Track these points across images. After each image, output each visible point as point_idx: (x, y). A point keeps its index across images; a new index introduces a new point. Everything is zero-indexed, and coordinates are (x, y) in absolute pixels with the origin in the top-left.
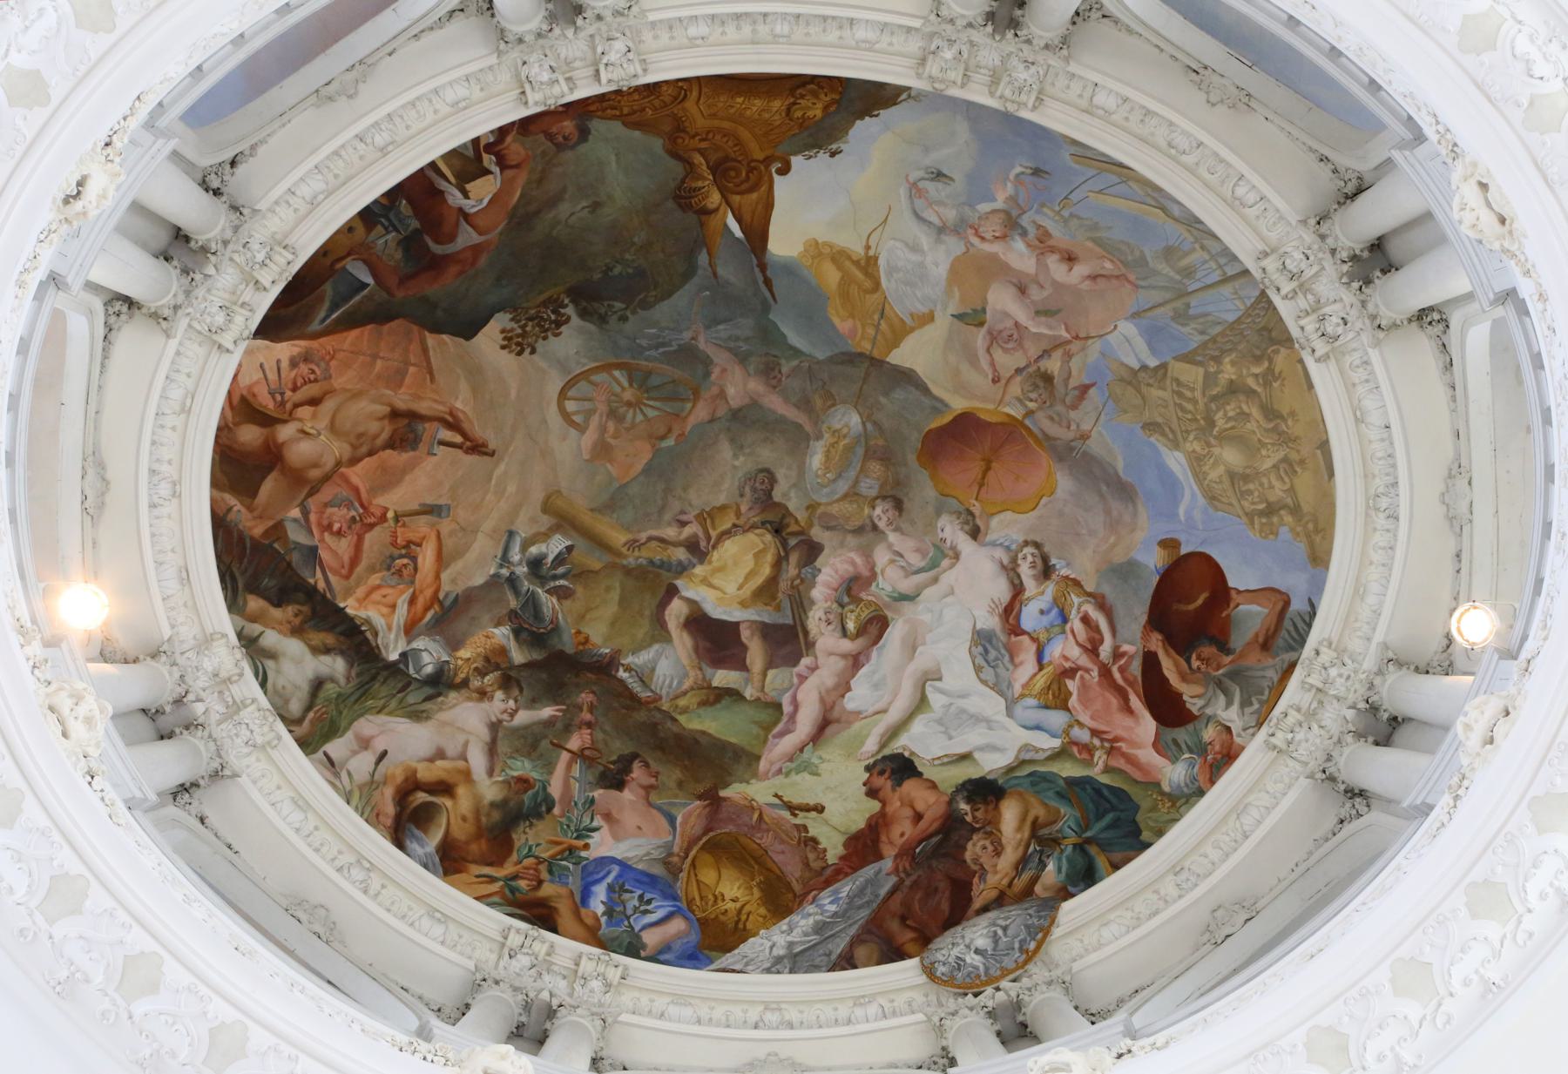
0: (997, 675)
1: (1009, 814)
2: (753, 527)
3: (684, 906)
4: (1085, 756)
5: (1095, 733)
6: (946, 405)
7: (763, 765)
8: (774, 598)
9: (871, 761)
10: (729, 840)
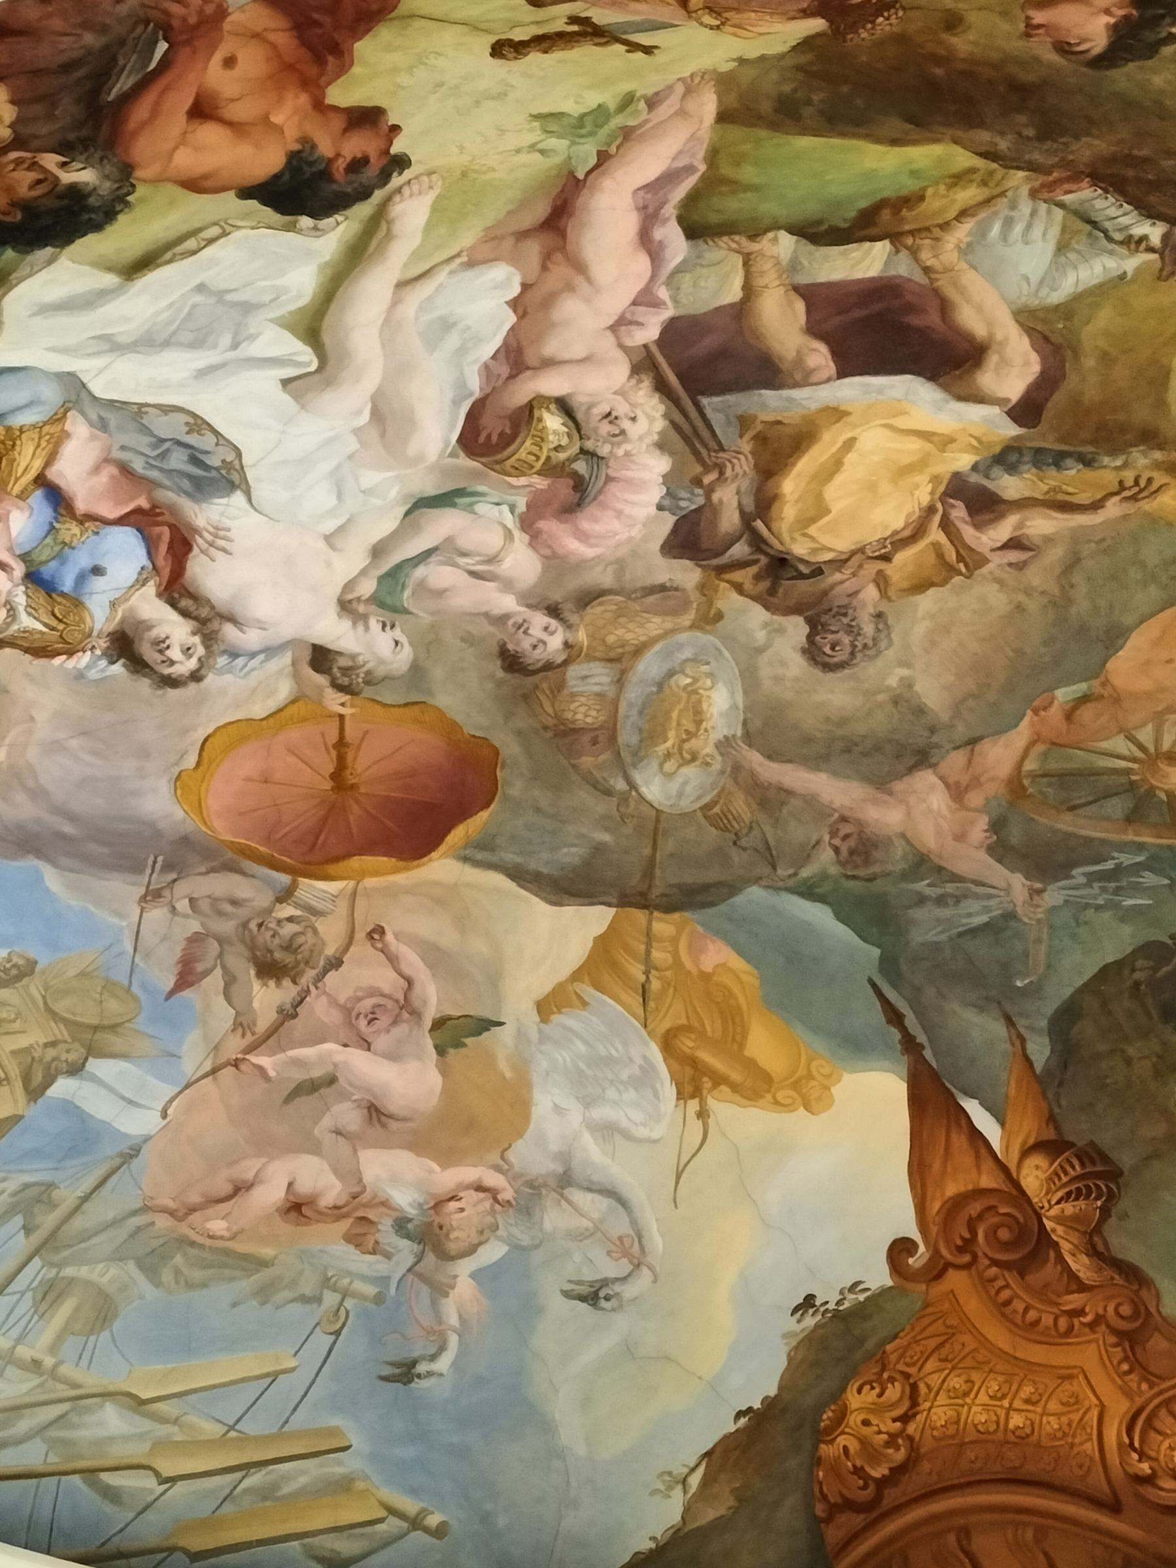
0: (146, 430)
2: (840, 563)
6: (465, 859)
8: (761, 440)
9: (396, 181)
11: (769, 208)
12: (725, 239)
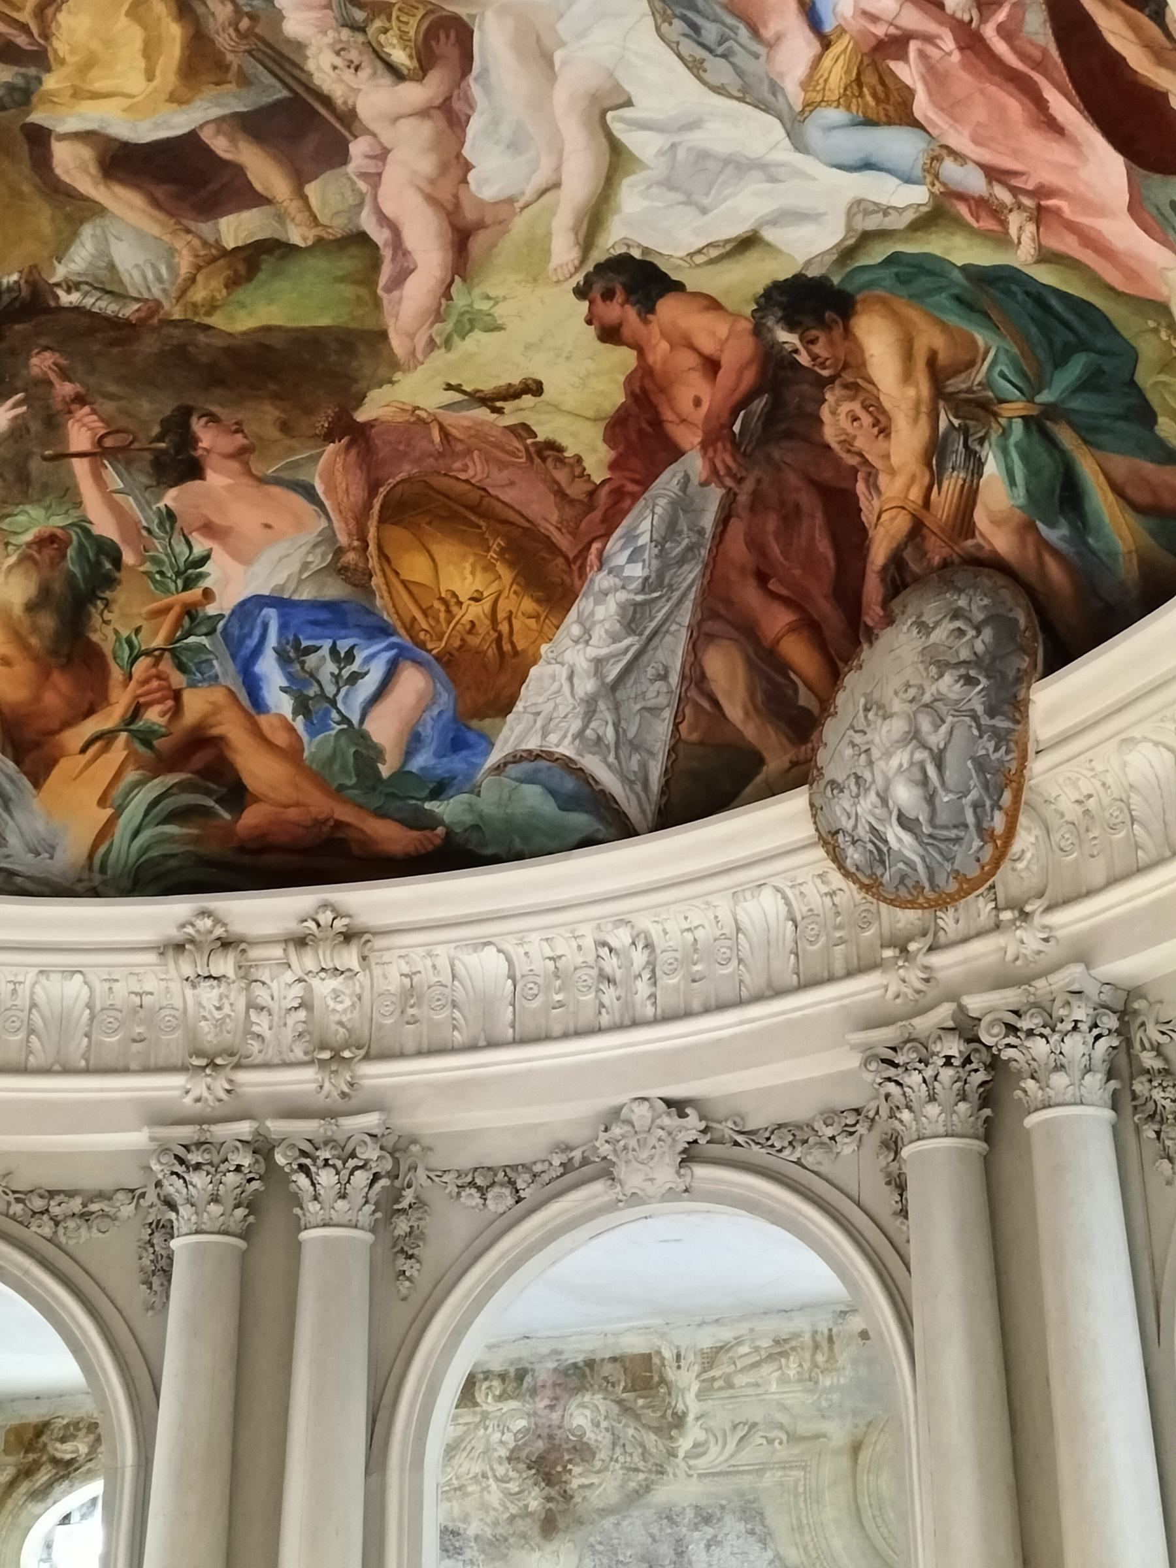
1: (877, 342)
3: (403, 638)
4: (988, 224)
5: (993, 174)
7: (398, 344)
9: (579, 278)
10: (418, 496)
11: (321, 263)
12: (339, 236)
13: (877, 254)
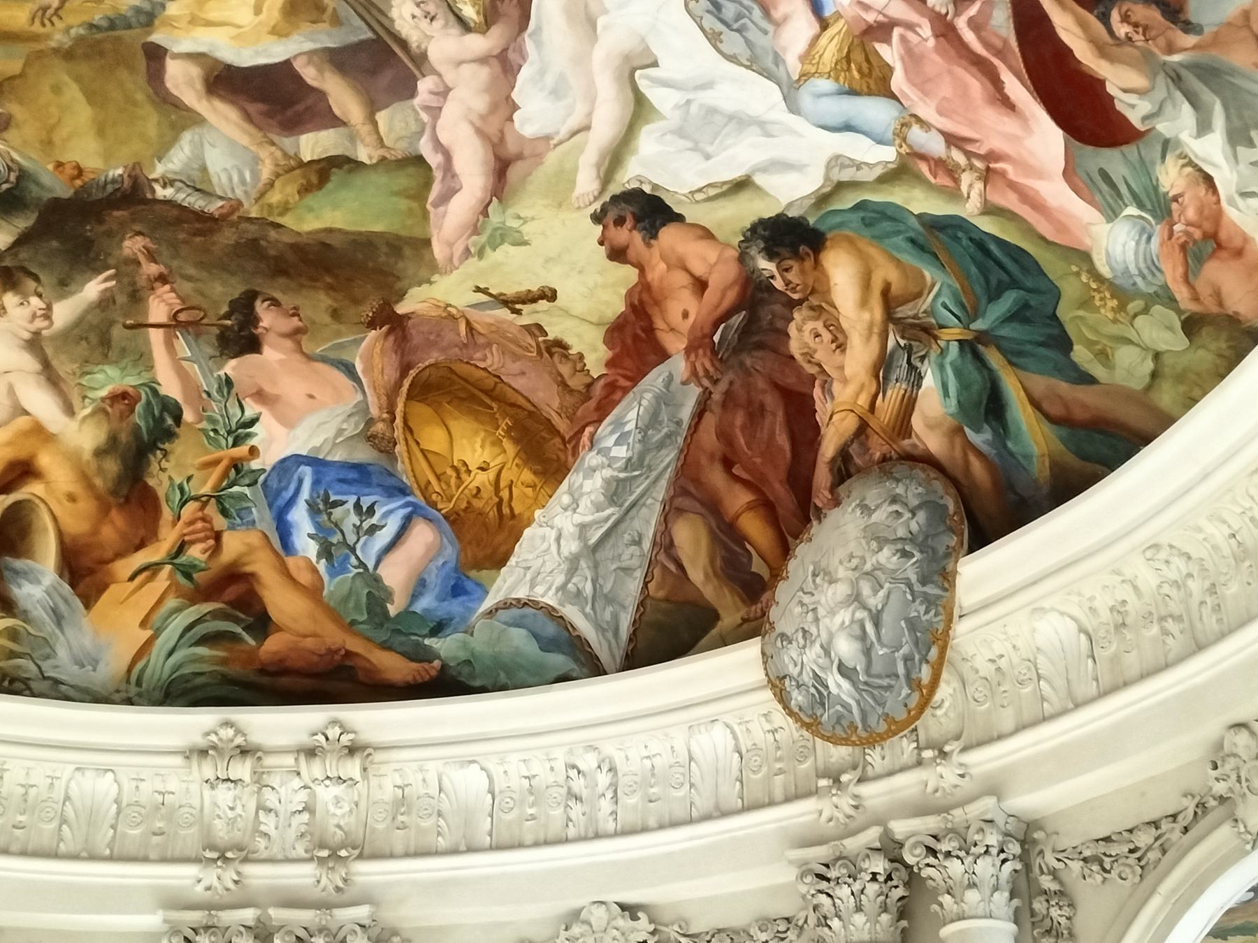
0: (748, 43)
1: (841, 273)
3: (418, 499)
4: (944, 180)
5: (952, 140)
7: (439, 251)
9: (597, 206)
10: (441, 380)
11: (380, 179)
13: (848, 201)
